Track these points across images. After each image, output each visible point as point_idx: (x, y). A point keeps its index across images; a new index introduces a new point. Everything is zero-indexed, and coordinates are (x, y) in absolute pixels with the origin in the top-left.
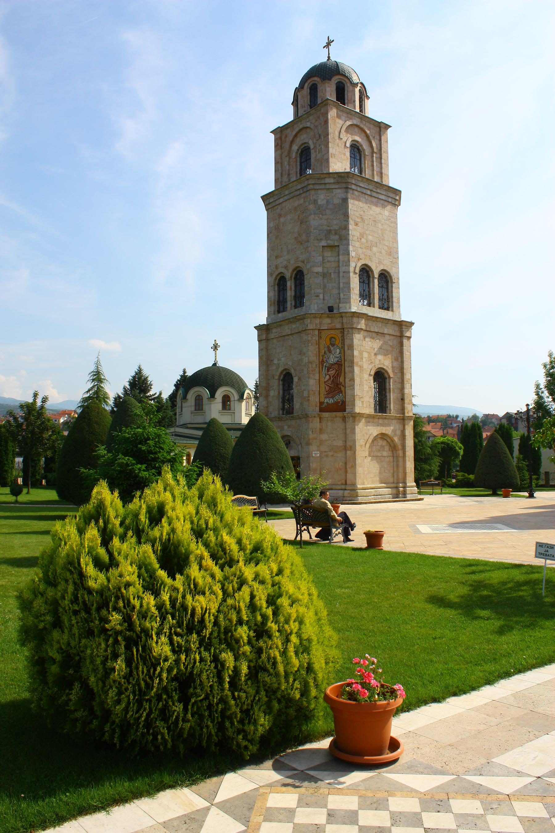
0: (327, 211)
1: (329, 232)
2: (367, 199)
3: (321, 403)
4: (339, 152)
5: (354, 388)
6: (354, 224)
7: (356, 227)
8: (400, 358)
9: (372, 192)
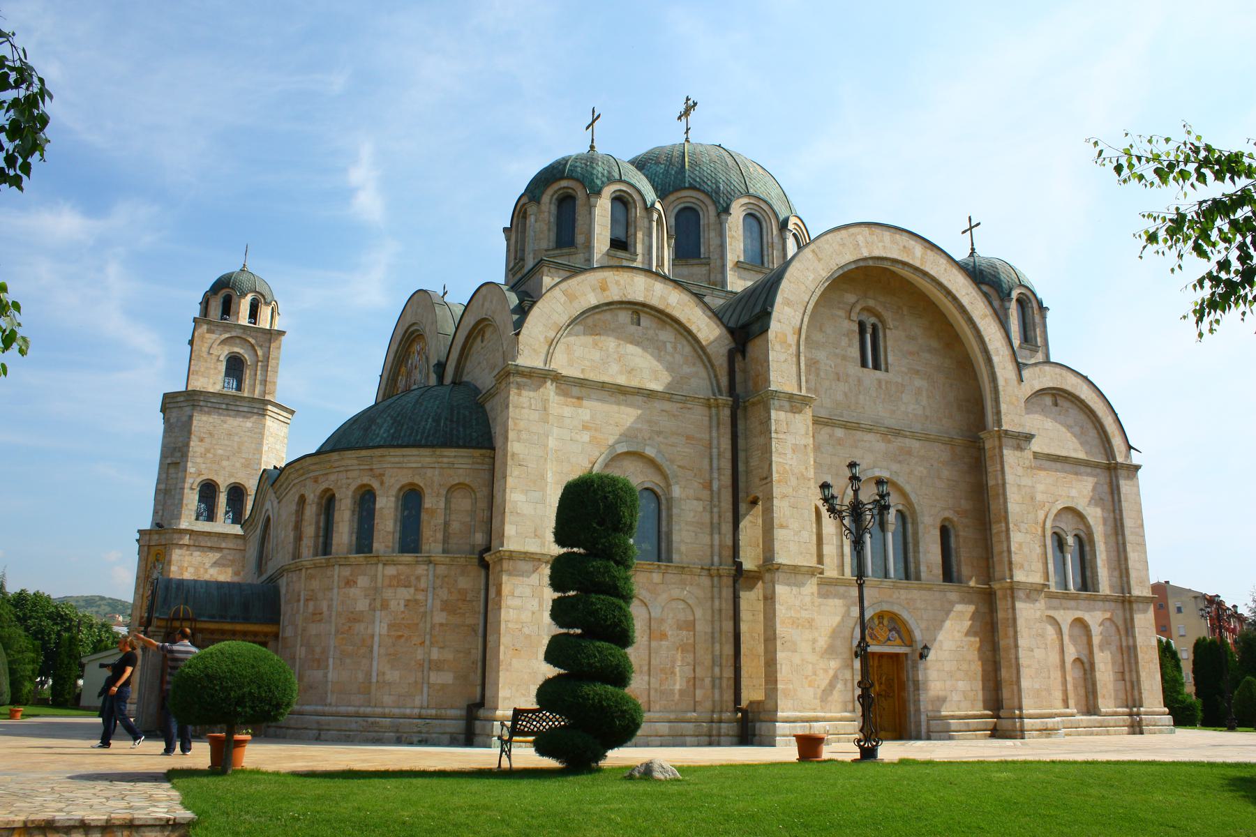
1: (175, 449)
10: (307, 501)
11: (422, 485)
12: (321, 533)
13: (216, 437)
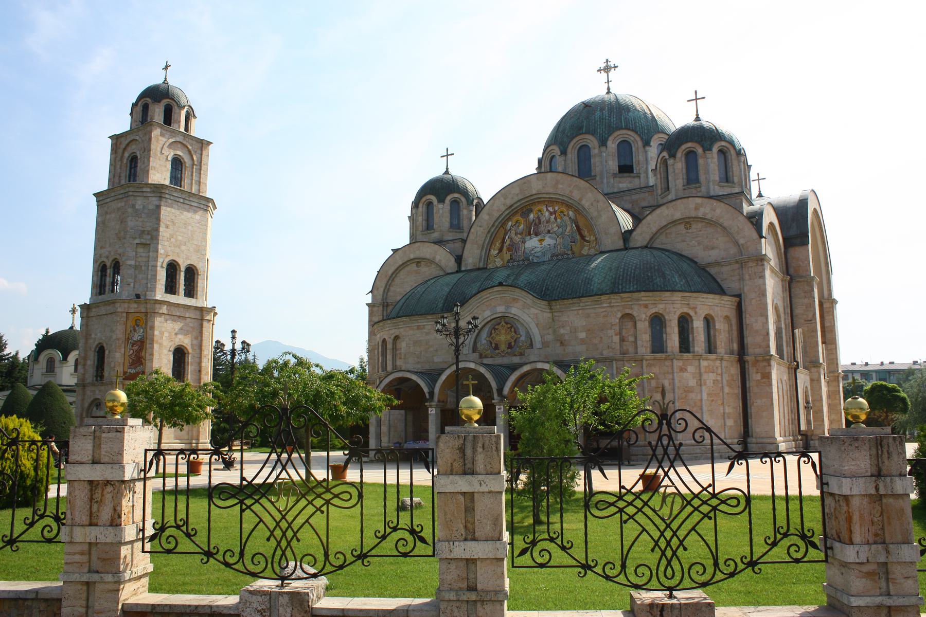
3: (125, 373)
4: (160, 165)
5: (153, 362)
8: (199, 338)
11: (713, 315)
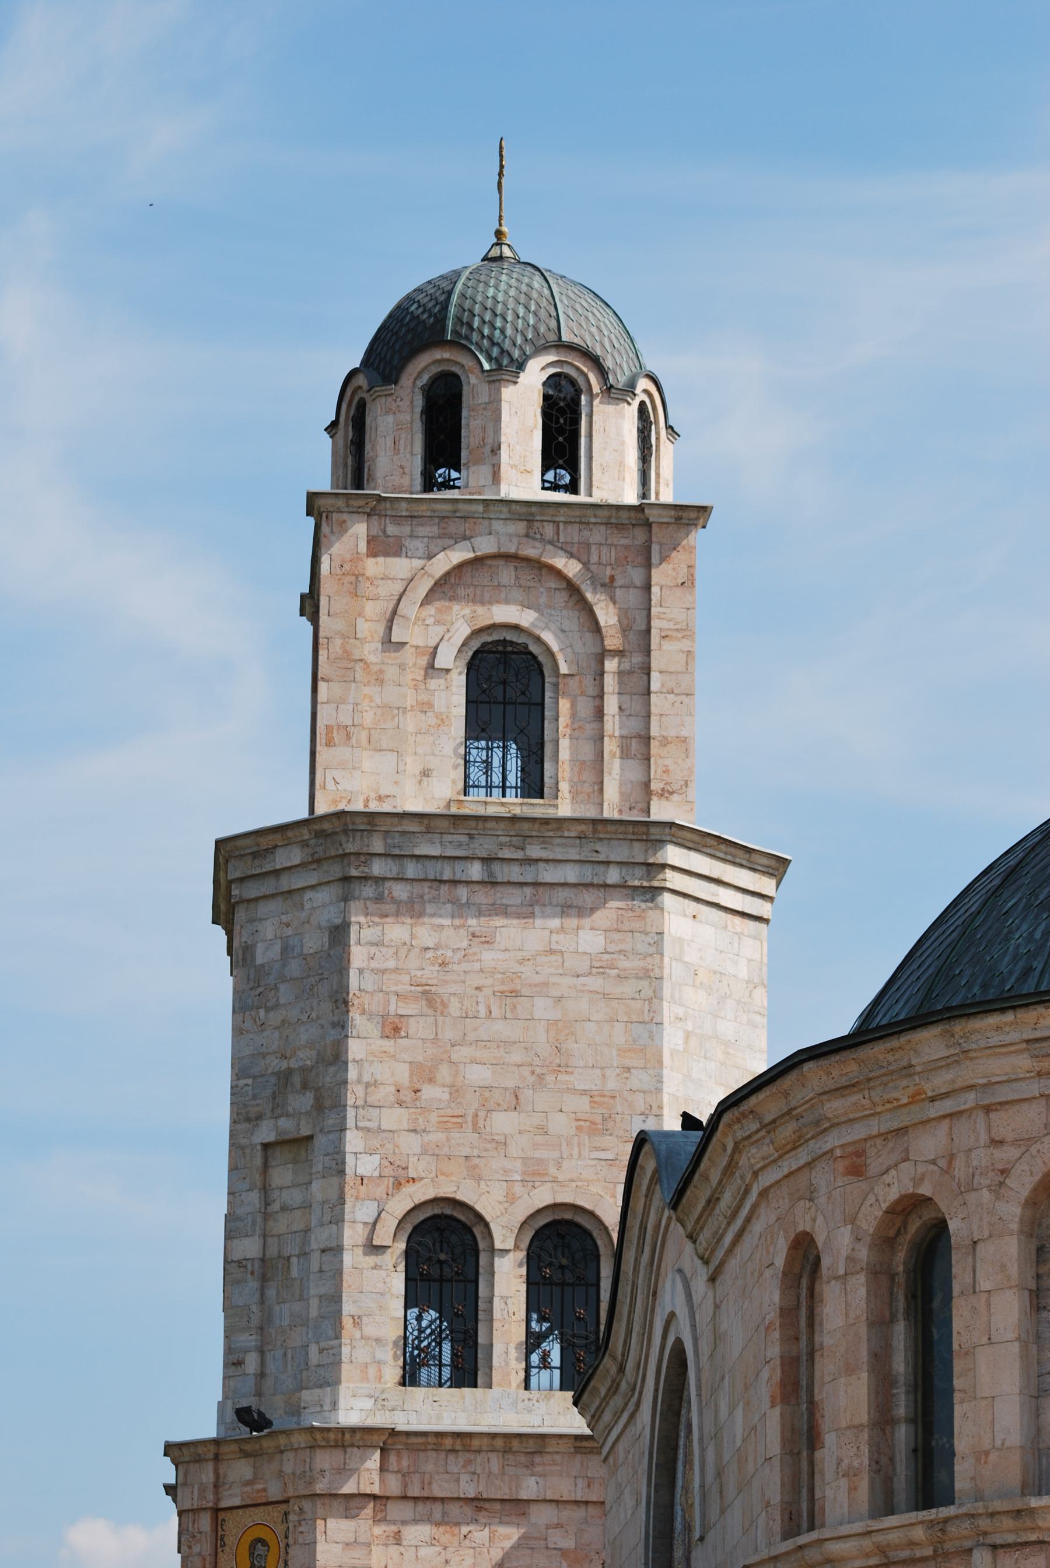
0: (282, 987)
1: (285, 1077)
2: (468, 904)
4: (386, 707)
6: (377, 1033)
7: (388, 1045)
9: (496, 867)
10: (826, 1262)
12: (901, 1409)
13: (454, 1008)
